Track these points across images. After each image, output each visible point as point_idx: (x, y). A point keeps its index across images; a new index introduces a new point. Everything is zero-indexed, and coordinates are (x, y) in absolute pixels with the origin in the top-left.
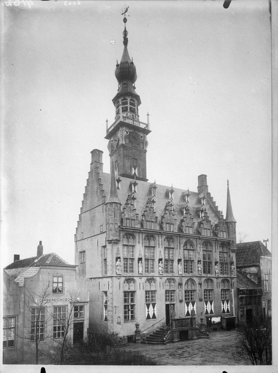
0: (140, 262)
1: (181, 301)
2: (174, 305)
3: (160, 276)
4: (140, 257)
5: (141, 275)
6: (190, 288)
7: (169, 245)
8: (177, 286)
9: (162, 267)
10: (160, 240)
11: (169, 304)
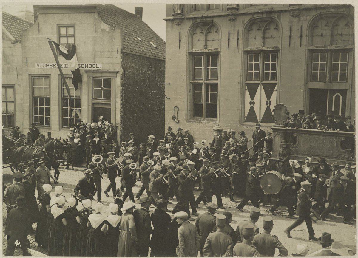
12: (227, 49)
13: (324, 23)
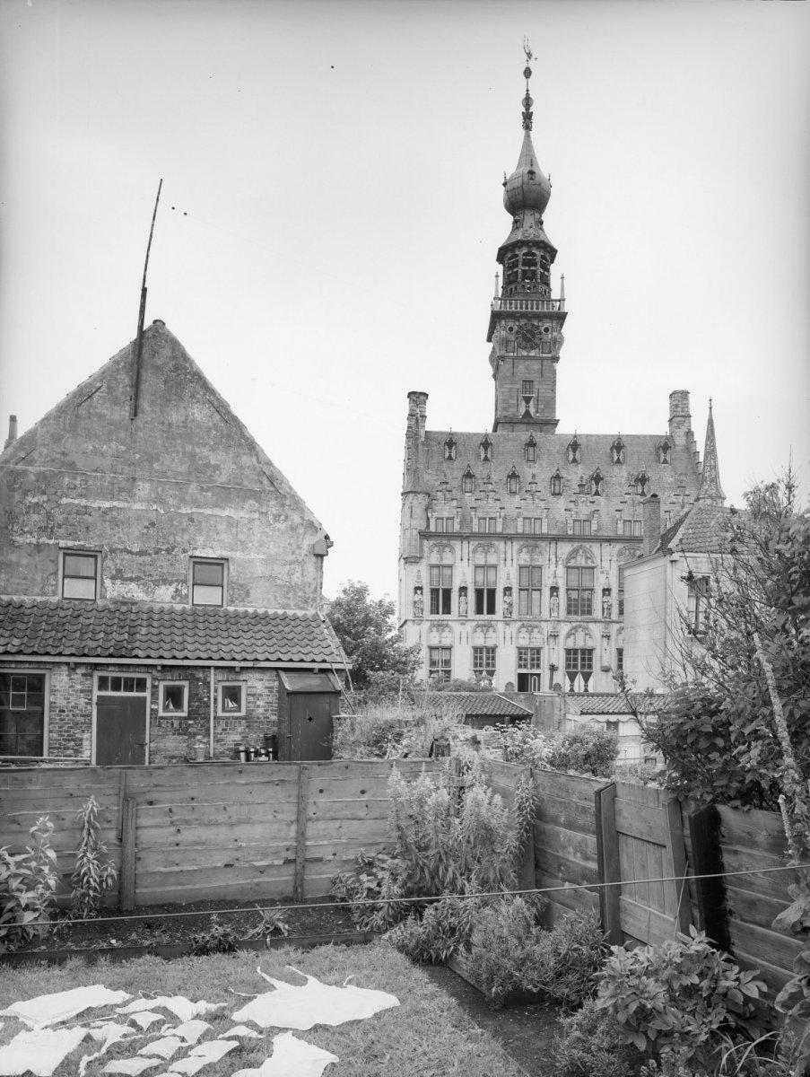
2: (538, 675)
5: (464, 618)
6: (580, 644)
7: (532, 559)
10: (509, 552)
11: (527, 674)
13: (525, 630)
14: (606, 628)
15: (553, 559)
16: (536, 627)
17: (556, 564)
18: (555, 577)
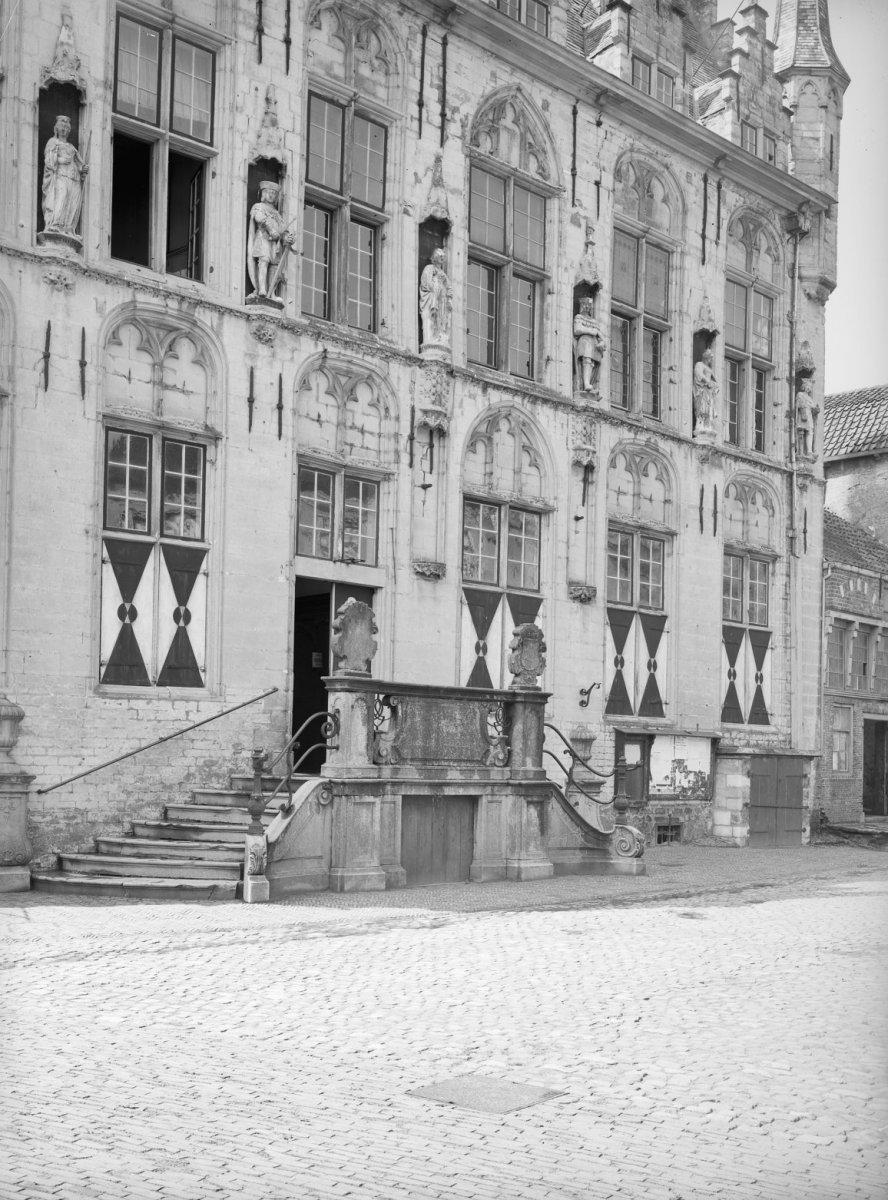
0: (62, 122)
1: (431, 573)
2: (367, 593)
3: (256, 310)
4: (62, 75)
6: (505, 489)
8: (404, 441)
9: (274, 232)
11: (327, 584)
12: (41, 391)
14: (589, 437)
15: (433, 108)
16: (369, 380)
17: (442, 128)
18: (438, 182)
